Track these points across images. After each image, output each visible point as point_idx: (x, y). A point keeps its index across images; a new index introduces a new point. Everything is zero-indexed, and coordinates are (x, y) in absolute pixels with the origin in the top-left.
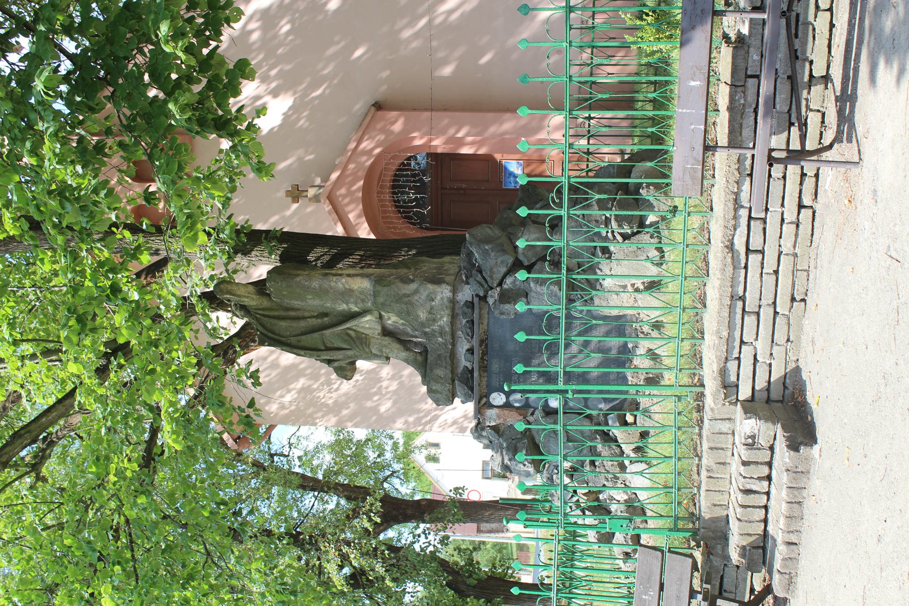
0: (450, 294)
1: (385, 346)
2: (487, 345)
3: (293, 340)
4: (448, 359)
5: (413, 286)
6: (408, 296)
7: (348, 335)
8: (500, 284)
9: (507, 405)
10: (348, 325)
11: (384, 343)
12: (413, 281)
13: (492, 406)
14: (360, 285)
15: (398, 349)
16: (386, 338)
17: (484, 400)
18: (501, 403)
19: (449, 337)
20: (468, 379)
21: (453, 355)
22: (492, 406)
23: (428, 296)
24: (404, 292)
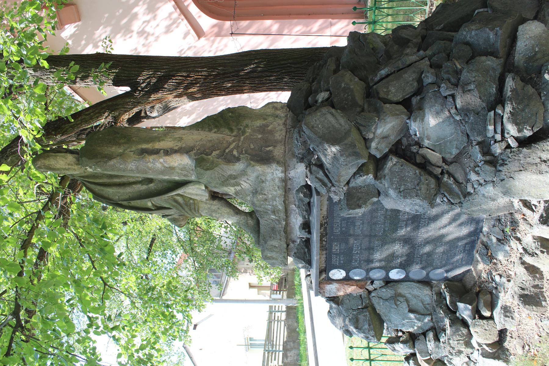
0: (281, 175)
1: (215, 211)
2: (326, 228)
3: (125, 203)
4: (282, 233)
5: (239, 166)
6: (235, 177)
7: (176, 201)
8: (348, 183)
9: (347, 280)
10: (174, 193)
11: (214, 208)
12: (238, 159)
13: (330, 281)
14: (180, 162)
15: (228, 213)
16: (215, 202)
17: (324, 276)
18: (341, 277)
19: (282, 215)
20: (305, 253)
21: (287, 230)
22: (330, 281)
23: (257, 177)
24: (229, 173)
